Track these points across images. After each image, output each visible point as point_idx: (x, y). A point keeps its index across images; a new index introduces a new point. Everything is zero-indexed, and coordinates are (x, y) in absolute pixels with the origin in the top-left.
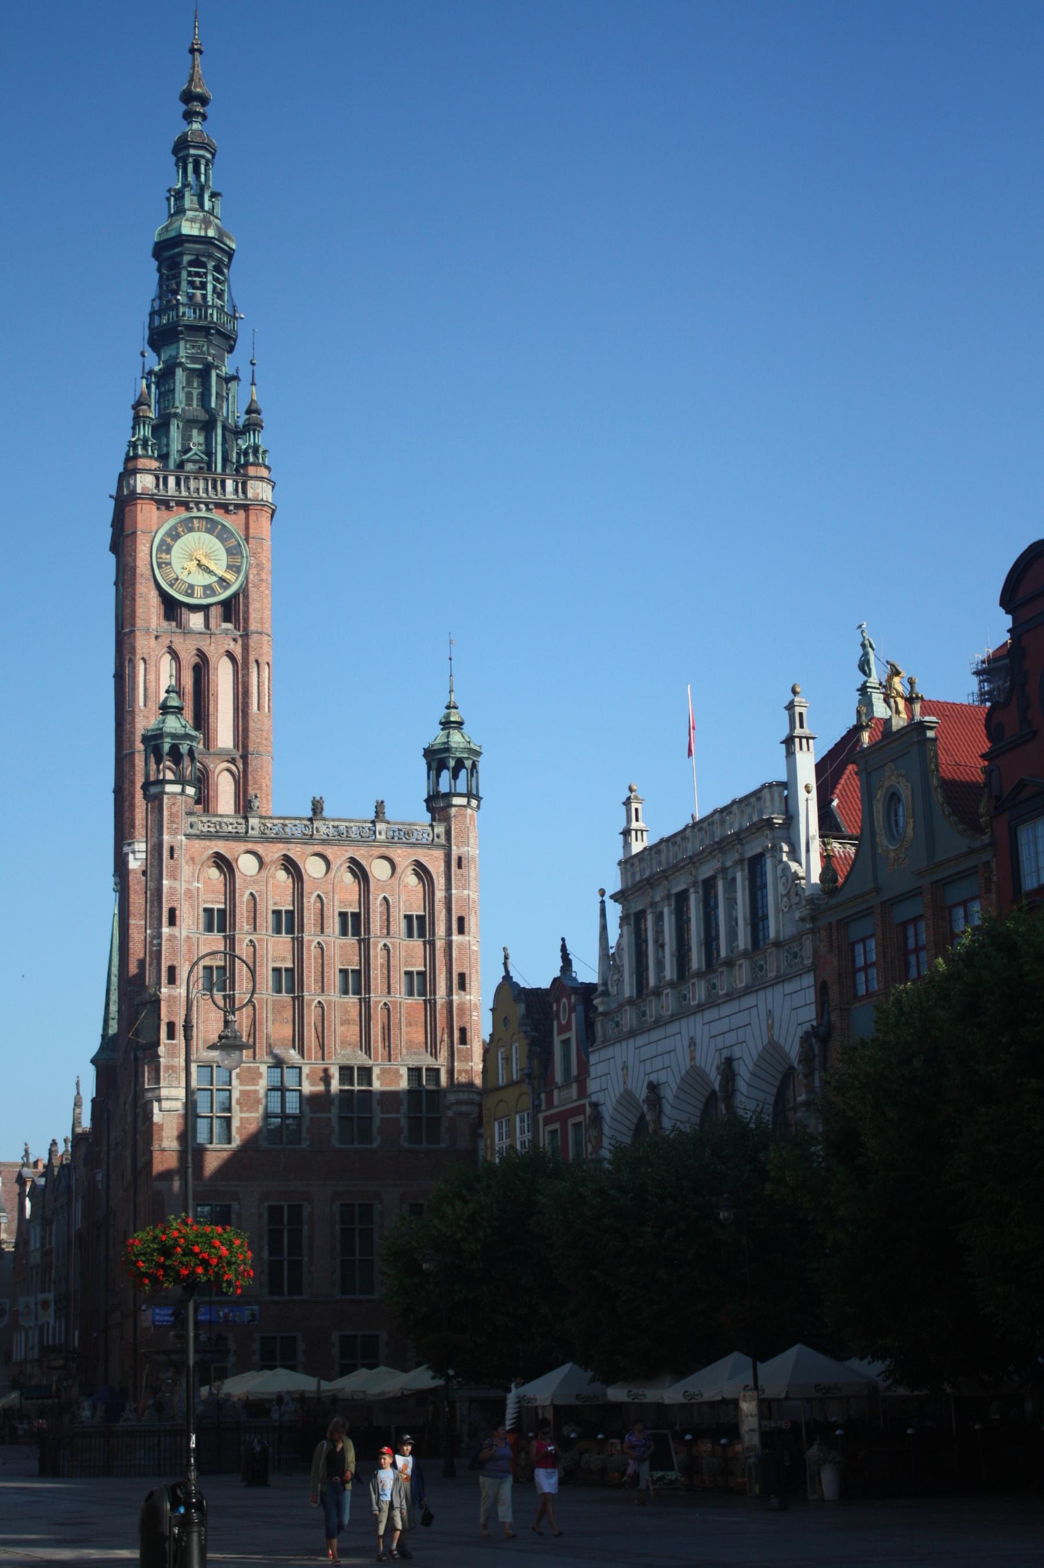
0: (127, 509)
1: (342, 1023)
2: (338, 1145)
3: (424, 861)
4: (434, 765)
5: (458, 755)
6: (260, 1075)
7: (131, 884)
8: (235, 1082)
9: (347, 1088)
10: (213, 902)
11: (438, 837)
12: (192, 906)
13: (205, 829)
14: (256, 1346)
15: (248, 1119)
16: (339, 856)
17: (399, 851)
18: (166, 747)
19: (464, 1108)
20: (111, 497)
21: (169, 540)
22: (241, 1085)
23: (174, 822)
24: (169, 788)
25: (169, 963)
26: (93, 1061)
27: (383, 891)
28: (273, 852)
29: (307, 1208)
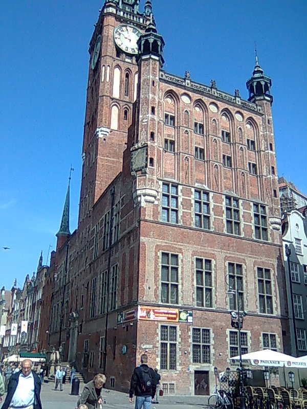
0: (105, 19)
1: (225, 179)
2: (226, 233)
3: (255, 118)
4: (255, 84)
5: (265, 80)
6: (192, 192)
7: (99, 143)
8: (180, 193)
9: (229, 207)
10: (168, 112)
11: (260, 110)
12: (161, 109)
13: (167, 79)
14: (191, 333)
15: (186, 212)
16: (222, 106)
17: (245, 112)
18: (151, 41)
19: (278, 226)
20: (94, 25)
21: (120, 31)
22: (183, 196)
23: (154, 71)
24: (153, 57)
25: (151, 131)
26: (57, 235)
27: (240, 125)
28: (196, 96)
29: (213, 262)
